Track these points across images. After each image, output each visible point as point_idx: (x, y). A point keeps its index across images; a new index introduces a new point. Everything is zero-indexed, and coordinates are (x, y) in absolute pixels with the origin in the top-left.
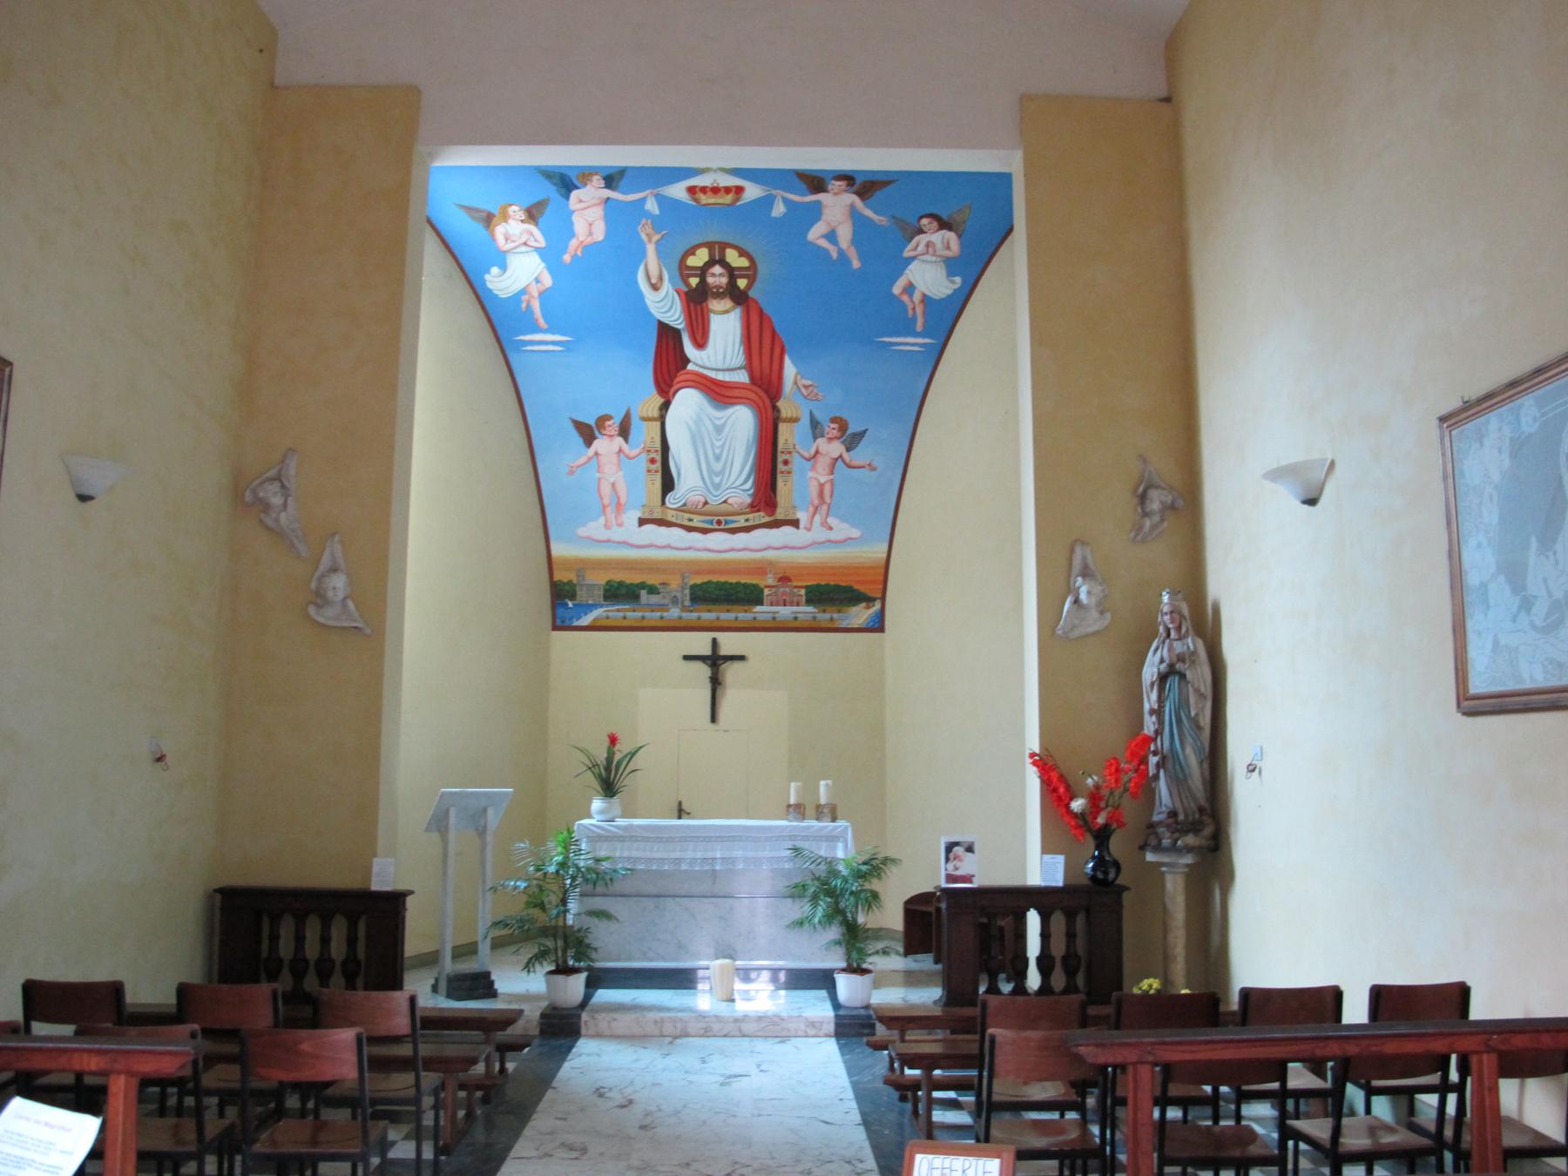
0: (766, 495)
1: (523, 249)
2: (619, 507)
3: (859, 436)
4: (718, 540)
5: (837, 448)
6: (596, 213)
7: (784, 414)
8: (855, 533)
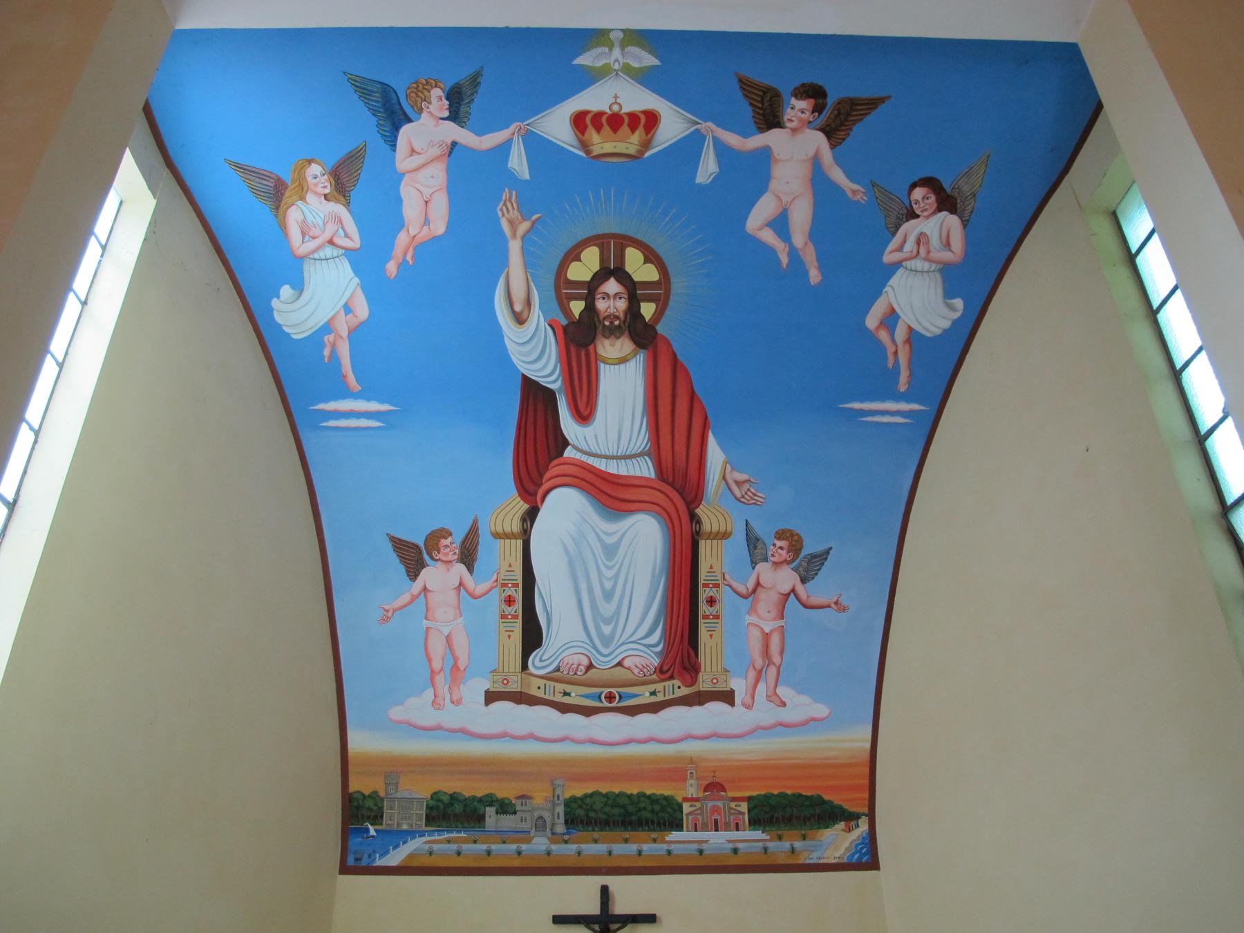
0: (682, 652)
1: (329, 251)
2: (457, 674)
3: (819, 559)
4: (610, 725)
5: (786, 579)
6: (436, 176)
7: (706, 527)
8: (821, 710)
